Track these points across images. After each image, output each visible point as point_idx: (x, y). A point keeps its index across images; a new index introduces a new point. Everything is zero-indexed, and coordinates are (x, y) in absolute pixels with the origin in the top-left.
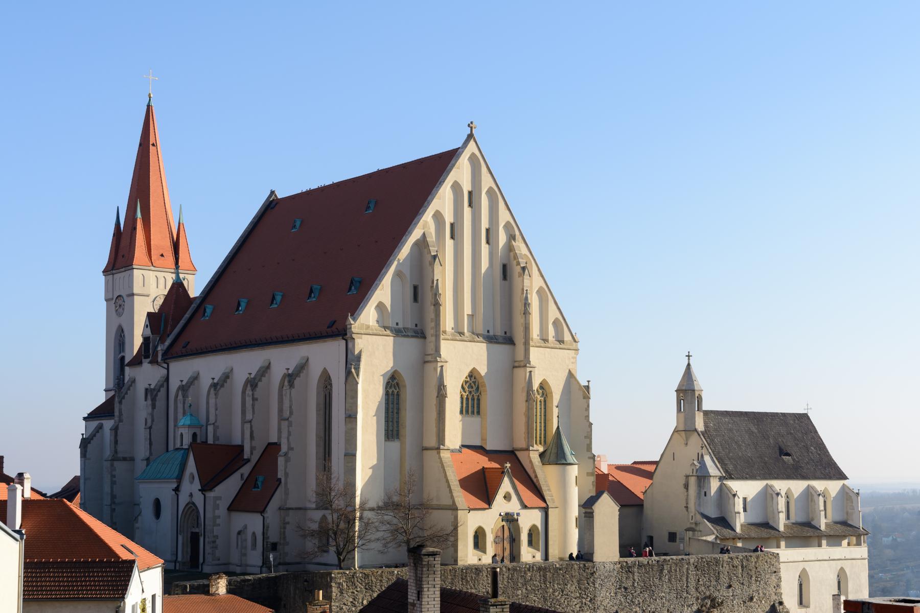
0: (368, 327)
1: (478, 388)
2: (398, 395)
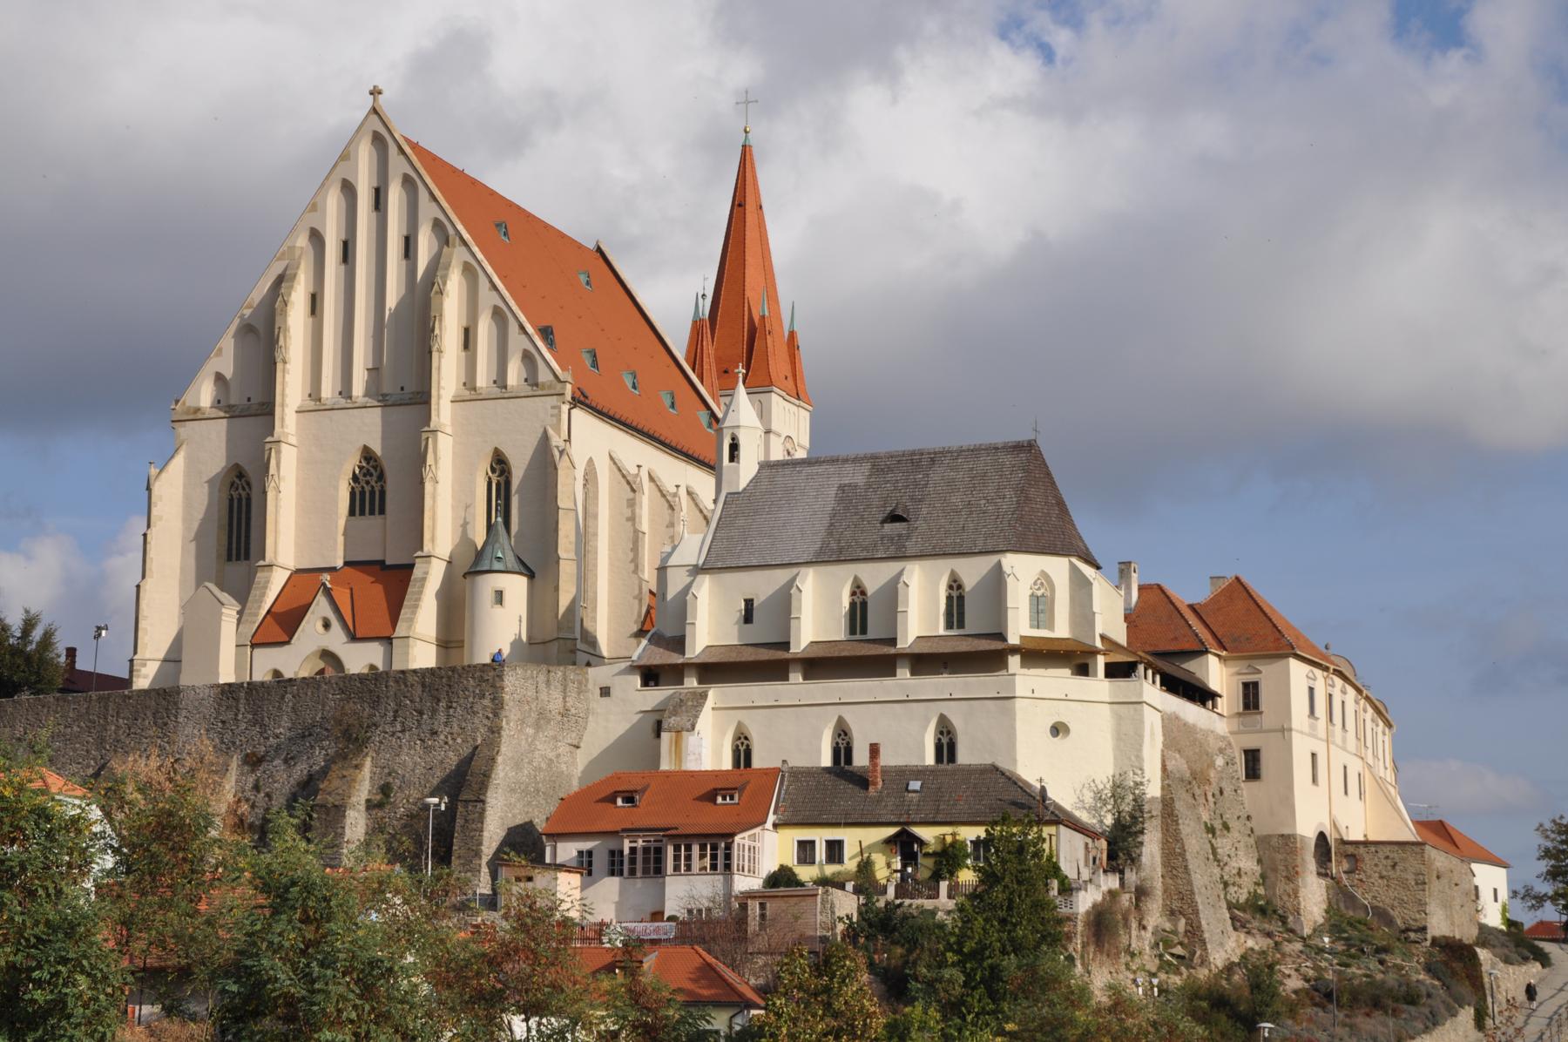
0: (198, 410)
1: (381, 477)
2: (249, 499)
